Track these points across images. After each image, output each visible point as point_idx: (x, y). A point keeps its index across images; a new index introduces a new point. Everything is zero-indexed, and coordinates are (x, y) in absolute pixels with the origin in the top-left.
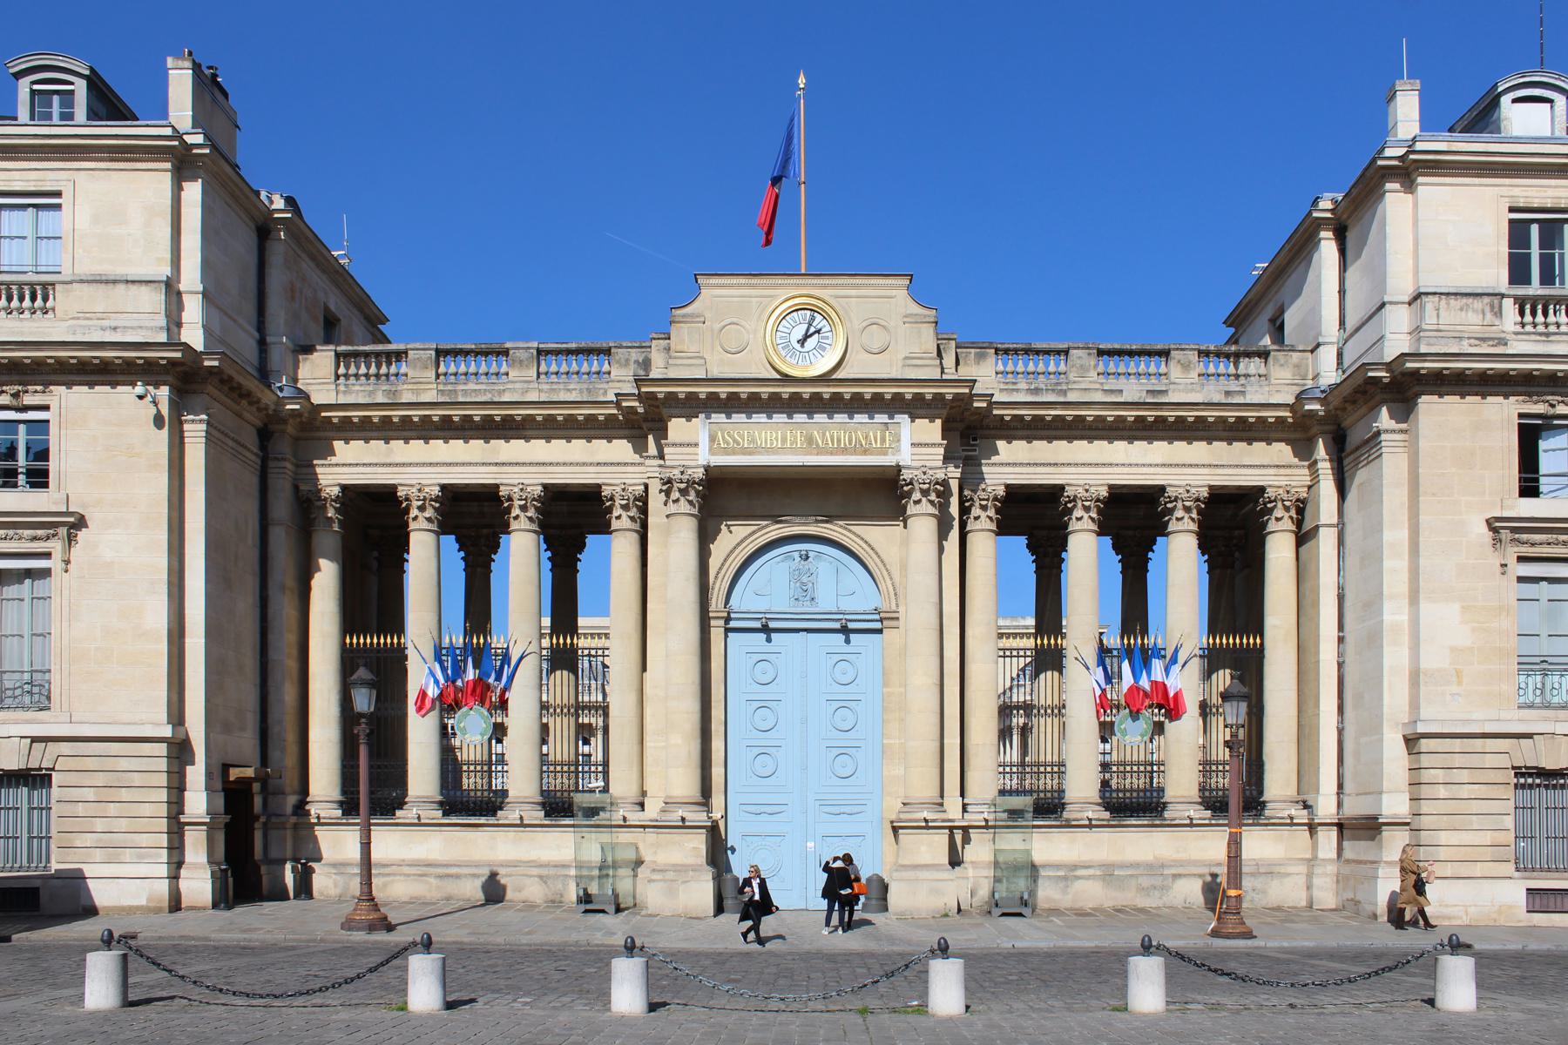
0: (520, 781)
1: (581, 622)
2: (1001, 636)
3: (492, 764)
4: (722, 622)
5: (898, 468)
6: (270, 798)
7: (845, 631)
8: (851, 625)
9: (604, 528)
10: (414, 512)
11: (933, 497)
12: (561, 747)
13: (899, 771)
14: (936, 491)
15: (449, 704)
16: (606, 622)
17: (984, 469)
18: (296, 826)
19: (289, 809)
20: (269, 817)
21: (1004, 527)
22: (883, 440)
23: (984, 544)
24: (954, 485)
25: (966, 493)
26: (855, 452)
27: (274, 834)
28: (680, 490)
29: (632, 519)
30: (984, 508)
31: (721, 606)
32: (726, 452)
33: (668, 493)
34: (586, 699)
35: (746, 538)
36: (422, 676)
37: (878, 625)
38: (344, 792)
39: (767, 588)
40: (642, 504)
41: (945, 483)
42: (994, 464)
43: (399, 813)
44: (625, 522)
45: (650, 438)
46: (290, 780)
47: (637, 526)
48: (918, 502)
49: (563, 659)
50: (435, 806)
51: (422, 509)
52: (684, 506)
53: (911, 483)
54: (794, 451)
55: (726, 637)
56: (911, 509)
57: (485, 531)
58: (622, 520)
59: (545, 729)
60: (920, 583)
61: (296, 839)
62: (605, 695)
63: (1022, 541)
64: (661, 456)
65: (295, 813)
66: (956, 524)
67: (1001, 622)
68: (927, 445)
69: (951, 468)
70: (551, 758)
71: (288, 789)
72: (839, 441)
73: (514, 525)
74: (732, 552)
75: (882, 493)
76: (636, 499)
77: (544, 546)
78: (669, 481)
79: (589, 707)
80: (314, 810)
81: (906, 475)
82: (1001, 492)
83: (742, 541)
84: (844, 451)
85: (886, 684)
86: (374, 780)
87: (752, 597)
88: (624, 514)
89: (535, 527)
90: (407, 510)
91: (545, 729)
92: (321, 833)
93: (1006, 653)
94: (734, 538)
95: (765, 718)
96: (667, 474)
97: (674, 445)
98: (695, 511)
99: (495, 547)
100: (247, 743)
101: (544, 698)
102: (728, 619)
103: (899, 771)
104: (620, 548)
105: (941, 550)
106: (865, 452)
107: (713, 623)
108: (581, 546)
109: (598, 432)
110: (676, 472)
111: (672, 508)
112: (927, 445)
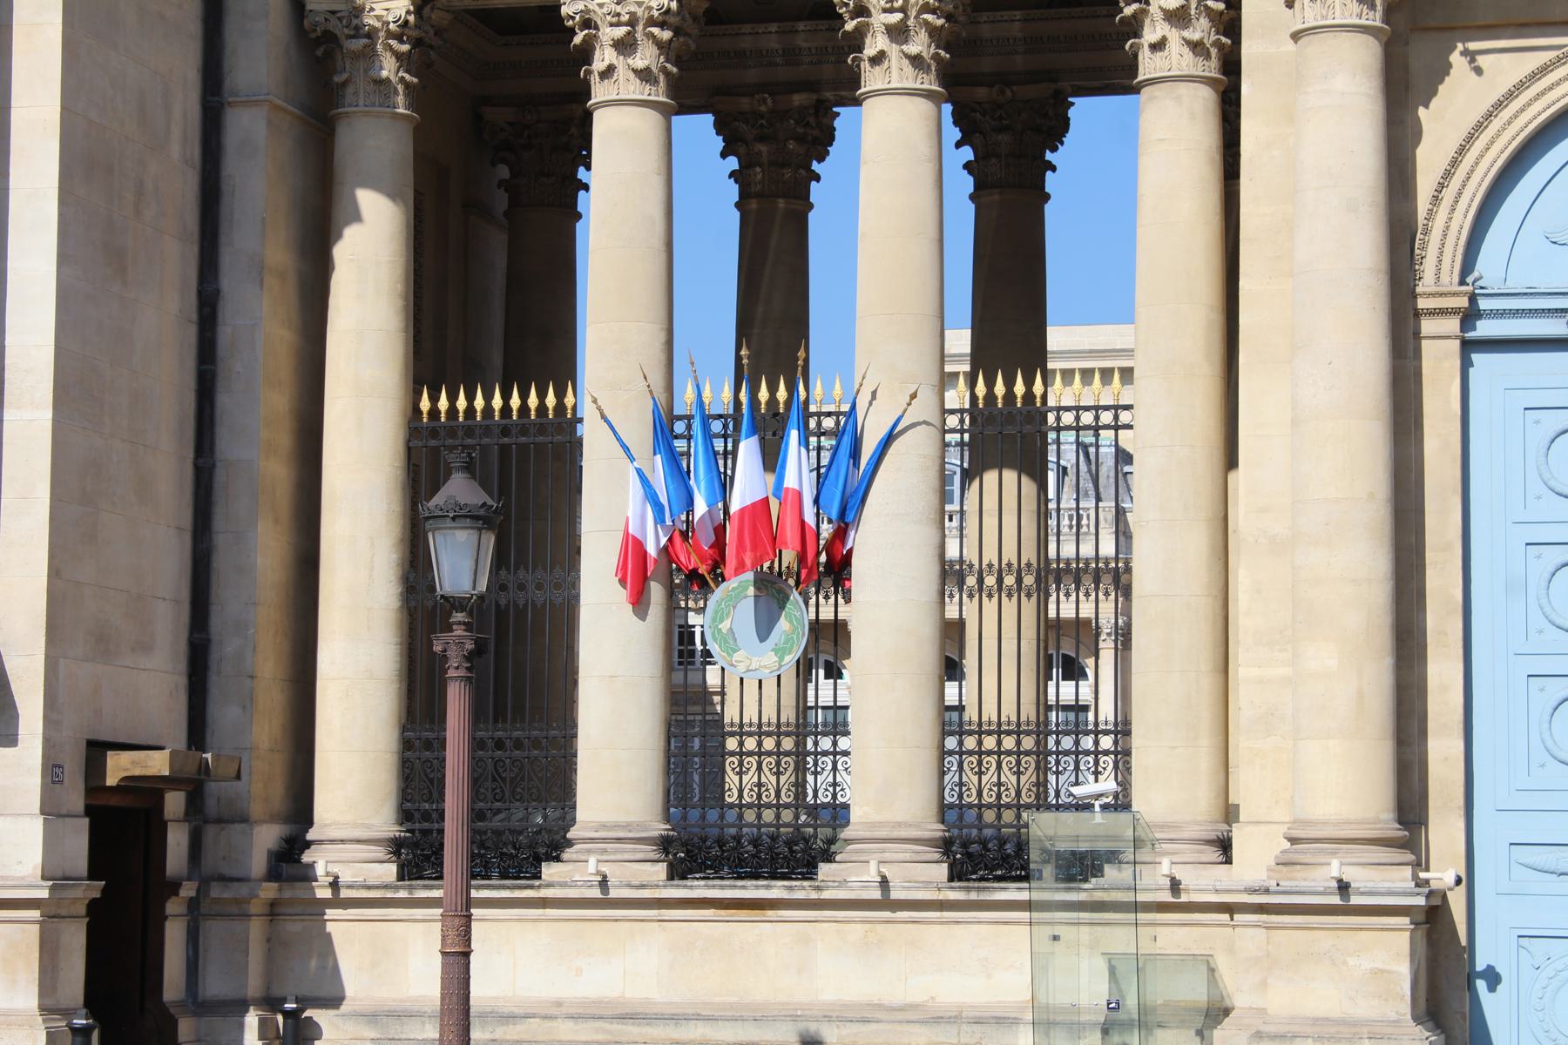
0: (884, 778)
1: (1057, 338)
3: (811, 731)
4: (1452, 325)
6: (210, 831)
9: (1119, 77)
10: (604, 56)
12: (998, 685)
15: (676, 575)
16: (1126, 330)
18: (274, 910)
19: (258, 863)
20: (205, 883)
27: (214, 931)
29: (1196, 47)
31: (1450, 278)
34: (1068, 550)
35: (1521, 86)
36: (615, 503)
38: (405, 816)
43: (549, 871)
44: (1178, 58)
46: (263, 785)
47: (1211, 68)
49: (1006, 438)
50: (649, 851)
51: (625, 46)
55: (1466, 364)
57: (798, 99)
59: (953, 632)
61: (272, 942)
62: (1123, 533)
65: (273, 875)
70: (971, 713)
71: (256, 809)
73: (872, 79)
74: (1479, 127)
77: (957, 134)
79: (1077, 574)
80: (322, 862)
83: (1510, 95)
86: (476, 782)
88: (1174, 36)
89: (930, 83)
90: (585, 54)
91: (953, 632)
92: (342, 929)
98: (1375, 19)
99: (821, 141)
100: (152, 689)
101: (952, 552)
102: (1470, 316)
107: (1428, 326)
108: (1056, 130)
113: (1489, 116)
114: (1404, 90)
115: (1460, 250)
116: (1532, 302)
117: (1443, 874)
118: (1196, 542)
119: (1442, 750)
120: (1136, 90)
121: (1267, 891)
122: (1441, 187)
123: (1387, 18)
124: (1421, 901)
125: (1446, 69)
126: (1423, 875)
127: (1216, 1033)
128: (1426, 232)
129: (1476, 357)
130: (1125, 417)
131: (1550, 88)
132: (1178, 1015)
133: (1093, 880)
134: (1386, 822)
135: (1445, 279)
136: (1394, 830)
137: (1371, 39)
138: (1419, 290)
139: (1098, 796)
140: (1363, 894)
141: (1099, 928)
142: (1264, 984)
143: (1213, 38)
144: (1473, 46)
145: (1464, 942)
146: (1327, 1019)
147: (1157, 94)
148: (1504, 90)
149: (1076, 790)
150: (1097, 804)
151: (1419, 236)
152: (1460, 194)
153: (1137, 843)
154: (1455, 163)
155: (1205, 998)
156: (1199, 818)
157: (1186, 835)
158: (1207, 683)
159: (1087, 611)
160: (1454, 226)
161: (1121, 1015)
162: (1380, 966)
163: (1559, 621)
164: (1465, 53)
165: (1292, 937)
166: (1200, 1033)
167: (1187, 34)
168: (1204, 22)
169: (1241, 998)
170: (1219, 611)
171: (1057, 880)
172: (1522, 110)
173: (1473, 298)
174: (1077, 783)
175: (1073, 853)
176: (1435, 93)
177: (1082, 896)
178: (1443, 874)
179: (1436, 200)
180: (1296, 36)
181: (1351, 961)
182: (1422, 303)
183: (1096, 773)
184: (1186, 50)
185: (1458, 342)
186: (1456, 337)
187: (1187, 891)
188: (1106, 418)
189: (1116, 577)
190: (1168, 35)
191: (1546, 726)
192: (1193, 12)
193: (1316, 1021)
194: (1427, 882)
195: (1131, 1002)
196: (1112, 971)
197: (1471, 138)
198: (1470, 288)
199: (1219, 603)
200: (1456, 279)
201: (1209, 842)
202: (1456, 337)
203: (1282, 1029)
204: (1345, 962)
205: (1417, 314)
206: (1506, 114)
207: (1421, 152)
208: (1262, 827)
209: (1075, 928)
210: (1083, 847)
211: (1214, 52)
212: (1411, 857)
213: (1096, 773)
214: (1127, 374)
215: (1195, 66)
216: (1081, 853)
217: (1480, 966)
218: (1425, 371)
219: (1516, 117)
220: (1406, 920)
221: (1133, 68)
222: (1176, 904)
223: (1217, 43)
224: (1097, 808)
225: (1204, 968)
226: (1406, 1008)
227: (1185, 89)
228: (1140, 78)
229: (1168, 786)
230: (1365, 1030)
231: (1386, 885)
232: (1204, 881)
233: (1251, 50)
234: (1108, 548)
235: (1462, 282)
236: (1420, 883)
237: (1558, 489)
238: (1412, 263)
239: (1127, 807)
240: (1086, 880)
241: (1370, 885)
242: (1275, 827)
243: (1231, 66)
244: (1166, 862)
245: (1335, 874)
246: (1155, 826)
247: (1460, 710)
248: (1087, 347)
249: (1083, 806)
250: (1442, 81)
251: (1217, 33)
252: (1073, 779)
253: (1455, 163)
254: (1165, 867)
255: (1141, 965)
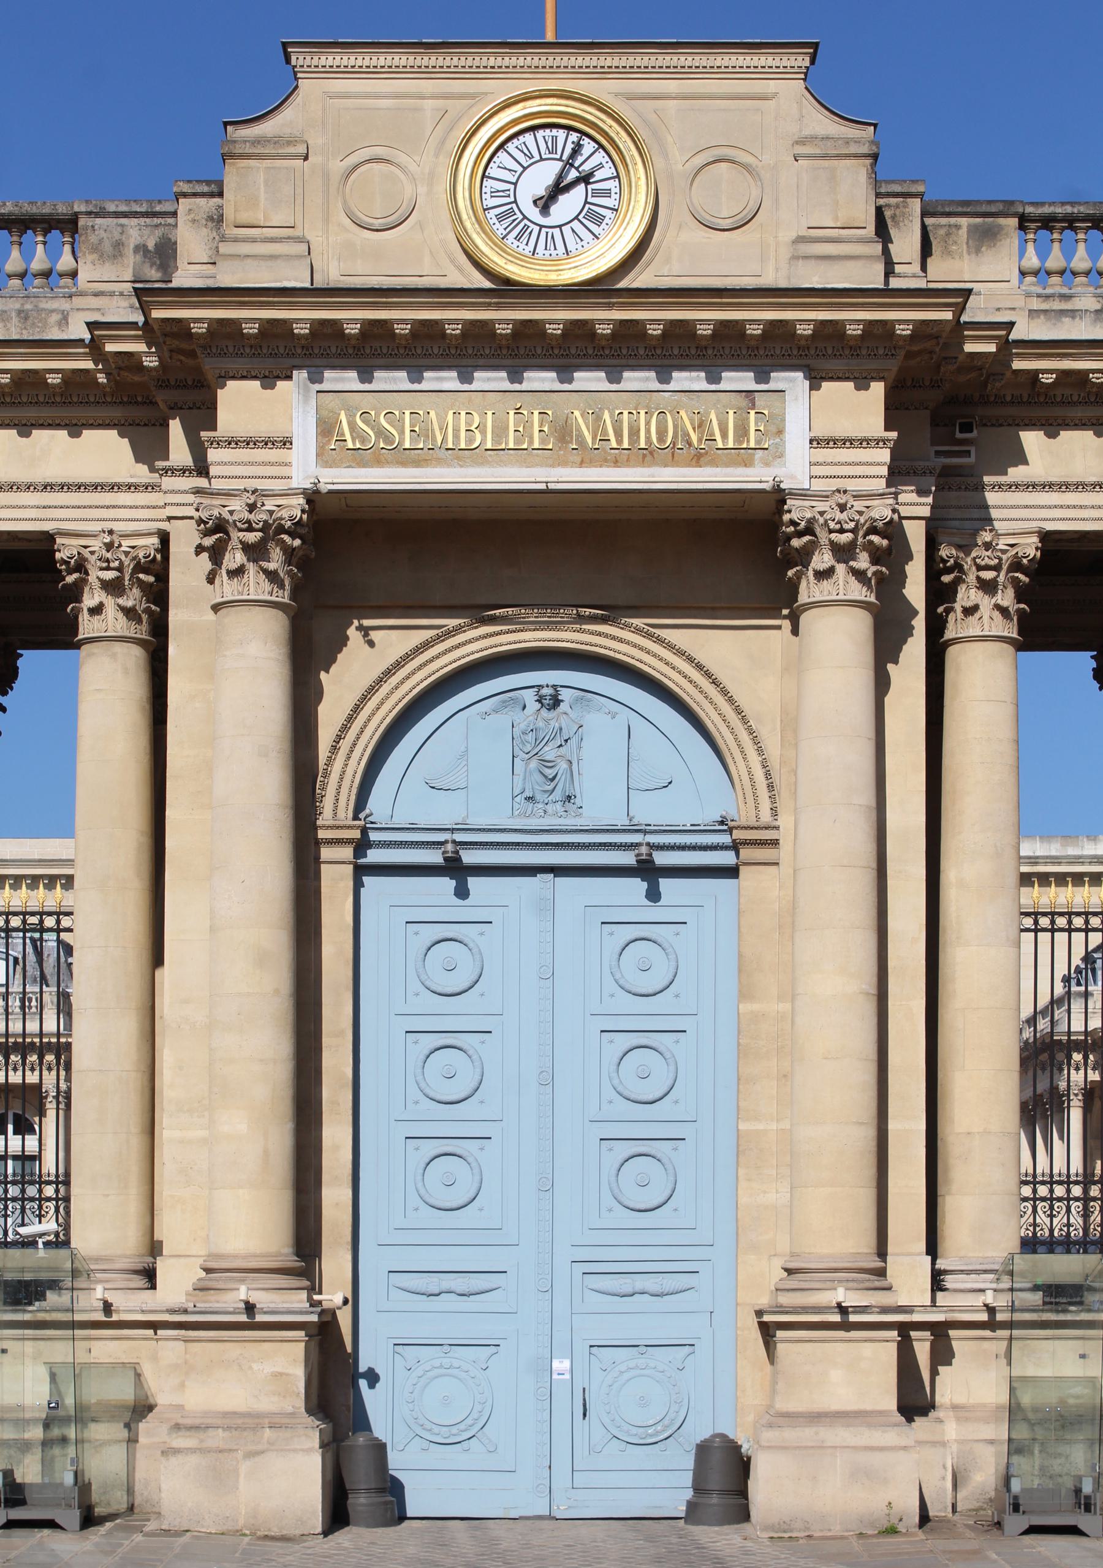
2: (1026, 879)
4: (347, 852)
5: (778, 497)
7: (647, 871)
8: (662, 859)
9: (63, 635)
11: (863, 562)
13: (776, 1195)
14: (870, 547)
17: (992, 498)
21: (1036, 632)
22: (742, 431)
23: (985, 671)
24: (916, 535)
25: (944, 552)
26: (672, 455)
28: (247, 548)
29: (130, 613)
30: (988, 587)
31: (345, 813)
32: (360, 457)
33: (216, 554)
37: (727, 858)
39: (461, 770)
40: (154, 577)
41: (893, 530)
42: (1015, 486)
44: (113, 621)
45: (175, 427)
47: (142, 631)
48: (825, 574)
52: (256, 585)
53: (809, 530)
54: (522, 454)
55: (358, 885)
56: (809, 590)
58: (104, 616)
60: (831, 758)
63: (1084, 661)
64: (202, 468)
66: (919, 624)
67: (1028, 849)
68: (848, 442)
69: (908, 495)
72: (634, 433)
74: (372, 690)
75: (739, 555)
76: (139, 568)
78: (220, 527)
81: (797, 511)
82: (1030, 548)
83: (398, 665)
84: (647, 456)
85: (745, 994)
87: (416, 796)
88: (110, 603)
93: (1040, 922)
94: (375, 659)
95: (450, 1073)
96: (214, 509)
97: (232, 442)
102: (362, 846)
103: (776, 1195)
104: (102, 680)
105: (882, 684)
106: (698, 458)
107: (326, 853)
109: (46, 413)
110: (237, 505)
111: (228, 589)
112: (848, 442)
113: (380, 681)
114: (308, 659)
115: (354, 791)
116: (411, 835)
117: (333, 1296)
118: (128, 1026)
119: (334, 1197)
120: (77, 646)
121: (185, 1311)
122: (339, 738)
123: (294, 596)
124: (314, 1318)
125: (344, 640)
126: (316, 1297)
127: (142, 1426)
128: (326, 775)
129: (365, 879)
130: (66, 922)
131: (431, 661)
132: (110, 1412)
133: (37, 1304)
134: (286, 1255)
135: (341, 814)
136: (292, 1262)
137: (281, 613)
138: (319, 823)
139: (41, 1235)
140: (265, 1313)
141: (42, 1343)
142: (182, 1385)
143: (144, 606)
144: (367, 623)
145: (349, 1349)
146: (235, 1413)
147: (96, 651)
148: (392, 660)
149: (23, 1231)
150: (40, 1241)
151: (319, 778)
152: (354, 745)
153: (75, 1273)
154: (351, 719)
155: (133, 1397)
156: (128, 1253)
157: (117, 1266)
158: (136, 1143)
159: (32, 1078)
160: (350, 771)
161: (60, 1412)
162: (279, 1369)
163: (432, 1095)
164: (360, 628)
165: (206, 1349)
166: (127, 1426)
167: (120, 601)
168: (136, 592)
169: (162, 1393)
170: (146, 1083)
171: (5, 1303)
172: (407, 678)
173: (364, 831)
174: (23, 1224)
175: (19, 1282)
176: (334, 660)
177: (27, 1317)
178: (333, 1296)
179: (334, 749)
180: (216, 608)
181: (255, 1366)
182: (322, 834)
183: (40, 1216)
184: (120, 615)
185: (351, 866)
186: (350, 863)
187: (118, 1311)
188: (50, 922)
189: (61, 1051)
190: (105, 602)
191: (420, 1177)
192: (127, 583)
193: (226, 1415)
194: (320, 1302)
195: (69, 1401)
196: (53, 1377)
197: (364, 699)
198: (362, 823)
199: (147, 1077)
200: (350, 814)
201: (136, 1272)
202: (350, 863)
203: (197, 1422)
204: (250, 1368)
205: (318, 843)
206: (394, 680)
207: (321, 709)
208: (182, 1260)
209: (20, 1343)
210: (28, 1277)
211: (145, 617)
212: (307, 1283)
213: (40, 1216)
214: (68, 882)
215: (129, 628)
216: (25, 1281)
217: (362, 1368)
218: (323, 890)
219: (402, 683)
220: (303, 1333)
221: (74, 627)
222: (109, 1321)
223: (147, 611)
224: (41, 1245)
225: (133, 1373)
226: (300, 1403)
227: (119, 648)
228: (80, 637)
229: (101, 1225)
230: (266, 1421)
231: (285, 1305)
232: (132, 1303)
233: (175, 617)
234: (50, 1025)
235: (356, 817)
236: (314, 1304)
237: (434, 988)
238: (314, 800)
239: (66, 1243)
240: (30, 1304)
241: (272, 1305)
242: (193, 1259)
243: (159, 630)
244: (99, 1288)
245: (243, 1297)
246: (91, 1259)
247: (349, 1166)
248: (36, 857)
249: (29, 1243)
250: (340, 651)
251: (148, 601)
252: (19, 1221)
253: (351, 719)
254: (99, 1292)
255: (78, 1372)
